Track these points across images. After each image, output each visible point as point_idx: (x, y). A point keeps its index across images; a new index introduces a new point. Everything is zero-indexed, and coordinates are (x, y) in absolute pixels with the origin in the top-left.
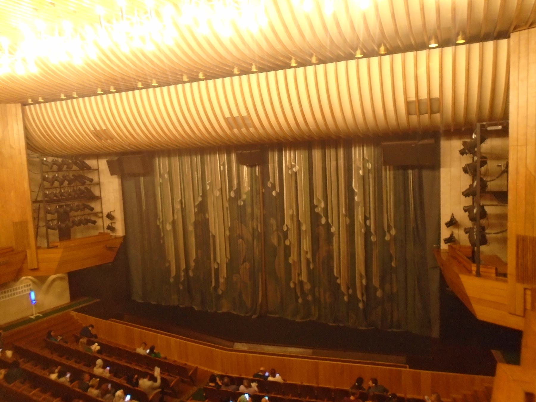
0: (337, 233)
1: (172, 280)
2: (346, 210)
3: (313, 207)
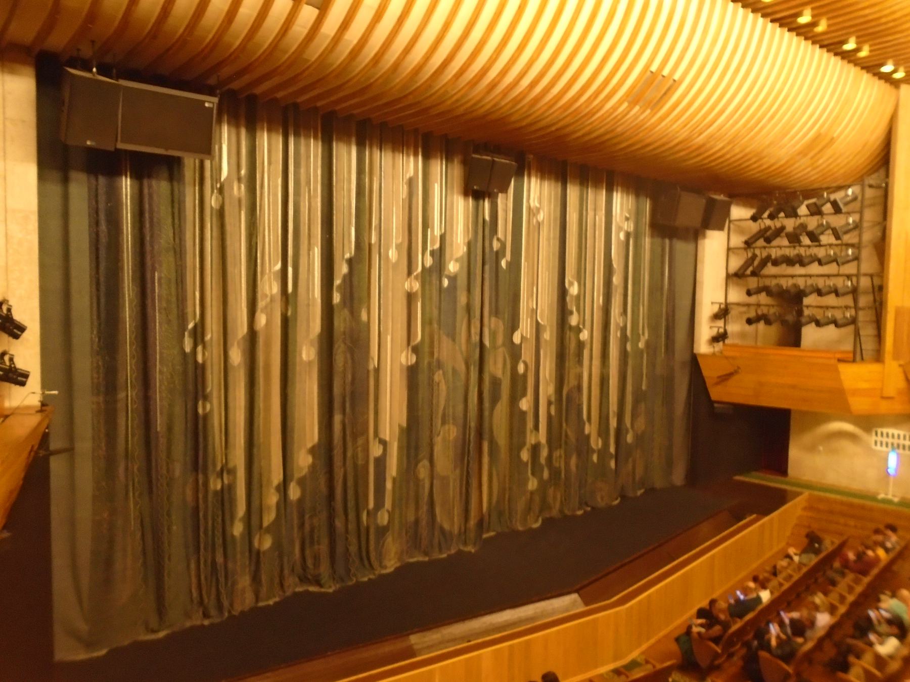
3: (563, 292)
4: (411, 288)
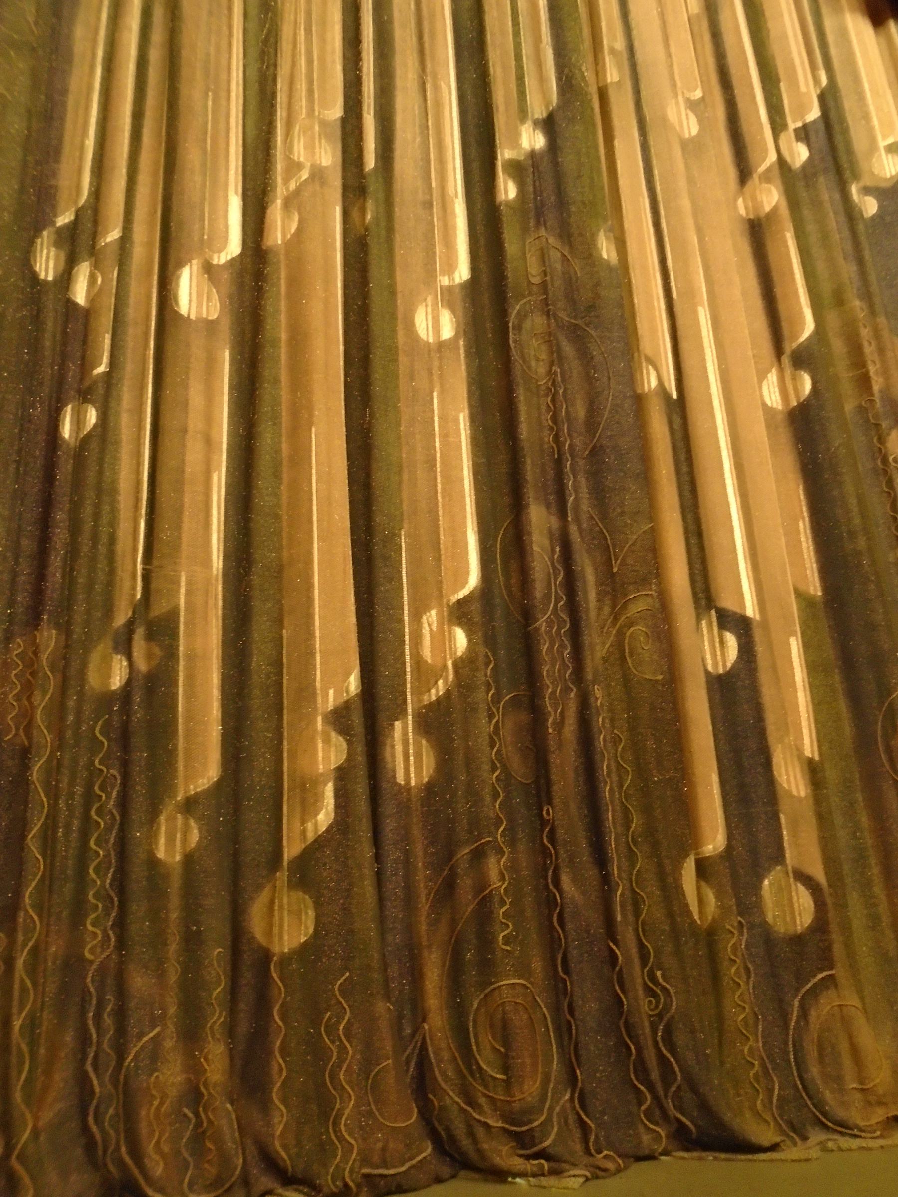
1: (173, 840)
4: (757, 206)
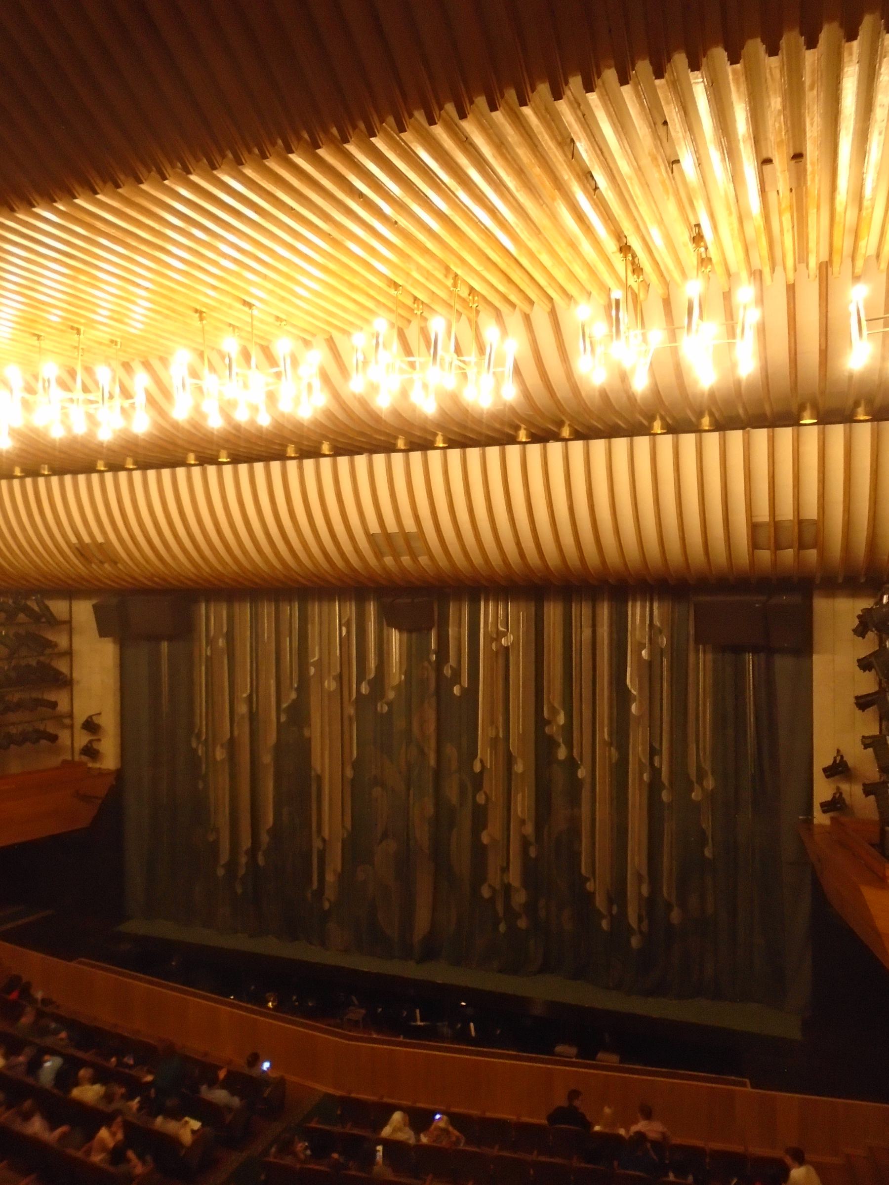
0: (588, 780)
1: (221, 872)
2: (611, 734)
3: (541, 722)
